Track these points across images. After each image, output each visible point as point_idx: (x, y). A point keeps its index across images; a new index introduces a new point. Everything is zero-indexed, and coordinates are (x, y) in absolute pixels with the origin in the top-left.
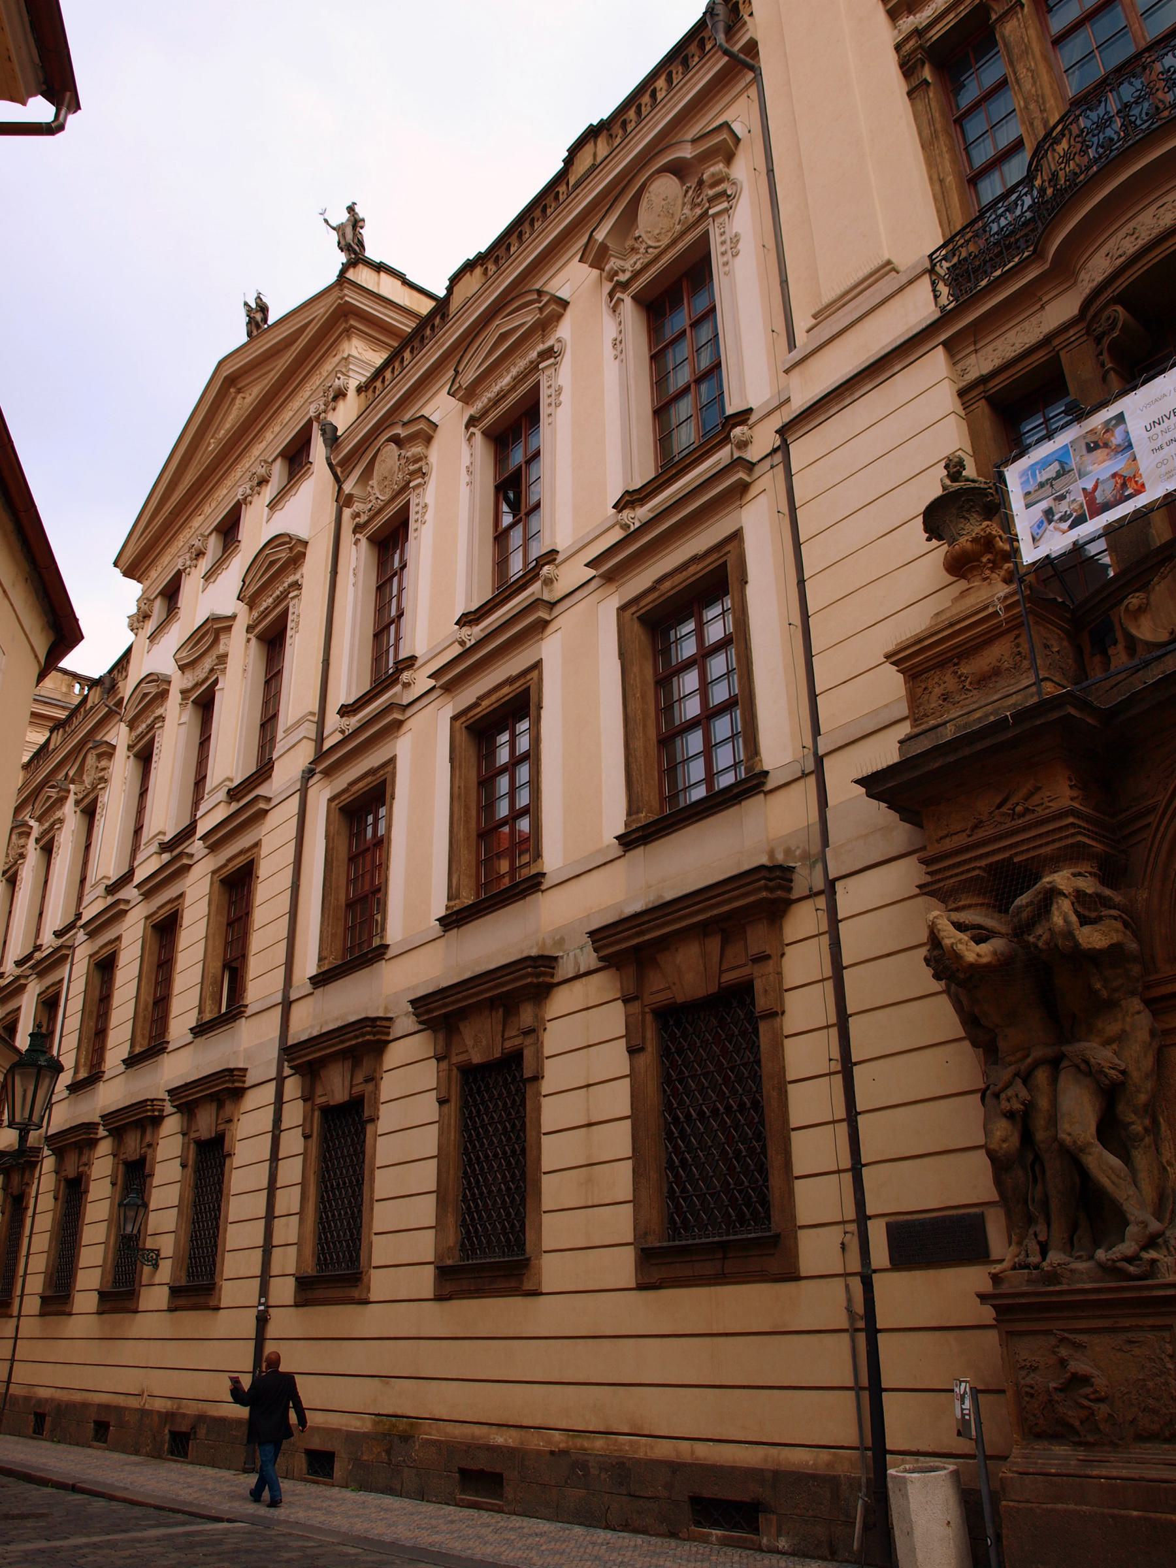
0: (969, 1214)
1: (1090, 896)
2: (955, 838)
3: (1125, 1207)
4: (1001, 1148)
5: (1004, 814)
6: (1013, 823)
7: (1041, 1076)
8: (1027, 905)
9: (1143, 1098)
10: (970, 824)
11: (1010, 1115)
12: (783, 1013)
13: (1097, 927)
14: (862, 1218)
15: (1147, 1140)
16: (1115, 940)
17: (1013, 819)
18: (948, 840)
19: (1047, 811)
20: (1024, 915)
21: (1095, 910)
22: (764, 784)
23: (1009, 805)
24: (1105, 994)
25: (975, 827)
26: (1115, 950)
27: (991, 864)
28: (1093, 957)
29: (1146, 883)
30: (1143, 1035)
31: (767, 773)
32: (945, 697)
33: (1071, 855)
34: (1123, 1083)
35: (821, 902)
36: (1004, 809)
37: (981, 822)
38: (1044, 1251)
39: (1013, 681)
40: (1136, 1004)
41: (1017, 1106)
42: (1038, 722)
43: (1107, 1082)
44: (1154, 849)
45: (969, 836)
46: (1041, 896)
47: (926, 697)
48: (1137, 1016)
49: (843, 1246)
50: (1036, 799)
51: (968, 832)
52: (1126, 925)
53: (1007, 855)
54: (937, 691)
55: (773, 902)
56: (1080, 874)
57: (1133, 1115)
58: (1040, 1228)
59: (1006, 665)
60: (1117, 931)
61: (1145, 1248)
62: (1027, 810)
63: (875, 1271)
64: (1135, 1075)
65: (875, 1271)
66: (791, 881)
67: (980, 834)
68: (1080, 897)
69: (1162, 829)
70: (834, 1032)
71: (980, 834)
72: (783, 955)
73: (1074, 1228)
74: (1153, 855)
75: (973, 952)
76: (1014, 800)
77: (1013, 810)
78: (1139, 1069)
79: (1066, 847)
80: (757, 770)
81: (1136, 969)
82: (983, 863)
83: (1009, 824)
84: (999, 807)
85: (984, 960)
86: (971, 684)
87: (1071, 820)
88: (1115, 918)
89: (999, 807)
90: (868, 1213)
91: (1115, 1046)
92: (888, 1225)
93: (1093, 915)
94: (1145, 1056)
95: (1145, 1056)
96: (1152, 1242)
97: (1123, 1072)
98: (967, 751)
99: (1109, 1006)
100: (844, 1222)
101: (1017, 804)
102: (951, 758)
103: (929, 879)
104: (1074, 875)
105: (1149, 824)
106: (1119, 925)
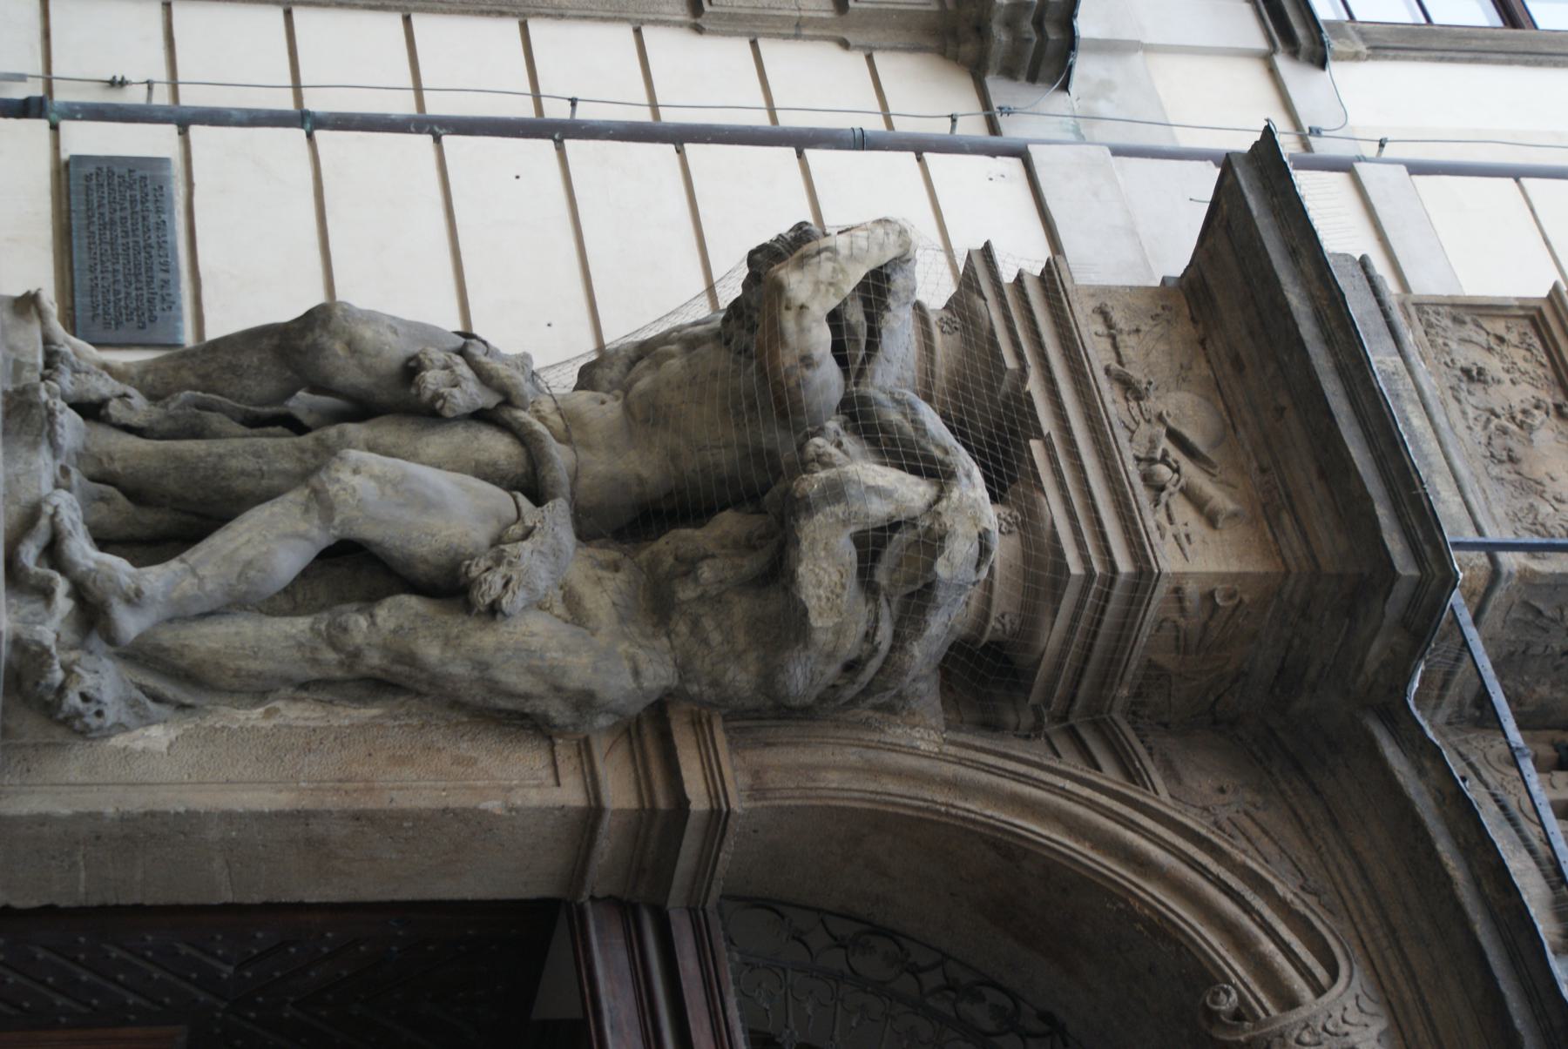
0: (179, 318)
1: (930, 567)
2: (1105, 344)
3: (174, 565)
4: (334, 335)
5: (1153, 443)
6: (1131, 466)
7: (497, 446)
8: (918, 424)
9: (431, 651)
10: (1136, 373)
11: (411, 369)
12: (698, 29)
13: (852, 582)
14: (184, 120)
15: (330, 656)
16: (816, 621)
17: (1138, 459)
18: (1101, 329)
19: (1155, 537)
20: (894, 416)
21: (893, 584)
22: (1294, 52)
23: (1175, 454)
24: (686, 592)
25: (1127, 385)
26: (787, 625)
27: (1031, 405)
28: (775, 570)
29: (952, 750)
30: (580, 668)
31: (1322, 64)
32: (1474, 376)
33: (1041, 568)
34: (469, 608)
35: (972, 127)
36: (1165, 443)
37: (1138, 398)
38: (91, 410)
39: (1499, 511)
40: (658, 674)
41: (433, 379)
42: (1383, 512)
43: (474, 572)
44: (1036, 773)
45: (1107, 371)
46: (938, 454)
47: (1481, 338)
48: (626, 665)
49: (117, 84)
50: (1184, 512)
51: (1115, 366)
52: (852, 667)
53: (1047, 423)
54: (1493, 365)
55: (981, 30)
56: (984, 550)
57: (391, 625)
58: (140, 409)
59: (1545, 509)
60: (839, 631)
61: (79, 591)
62: (1157, 488)
63: (54, 128)
64: (486, 639)
65: (54, 128)
66: (1033, 78)
67: (1109, 394)
68: (932, 543)
69: (1086, 792)
70: (643, 116)
71: (1109, 394)
72: (845, 45)
73: (137, 494)
74: (1022, 769)
75: (812, 293)
76: (1187, 466)
77: (1164, 460)
78: (499, 649)
79: (1059, 553)
80: (1335, 45)
81: (741, 678)
82: (1034, 386)
83: (1127, 454)
84: (1174, 436)
85: (789, 322)
86: (1504, 431)
87: (1124, 565)
88: (869, 636)
89: (1174, 436)
90: (196, 131)
91: (559, 609)
92: (162, 163)
93: (881, 576)
94: (531, 670)
95: (531, 670)
96: (92, 614)
97: (494, 611)
98: (1321, 360)
99: (657, 605)
100: (174, 84)
101: (1177, 471)
102: (1307, 330)
103: (1008, 277)
104: (984, 537)
105: (1098, 768)
106: (851, 646)
